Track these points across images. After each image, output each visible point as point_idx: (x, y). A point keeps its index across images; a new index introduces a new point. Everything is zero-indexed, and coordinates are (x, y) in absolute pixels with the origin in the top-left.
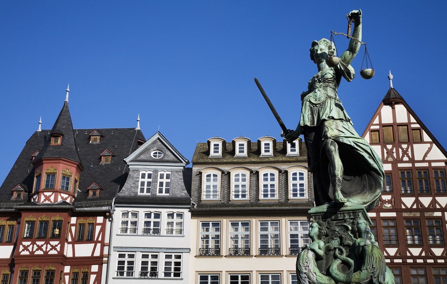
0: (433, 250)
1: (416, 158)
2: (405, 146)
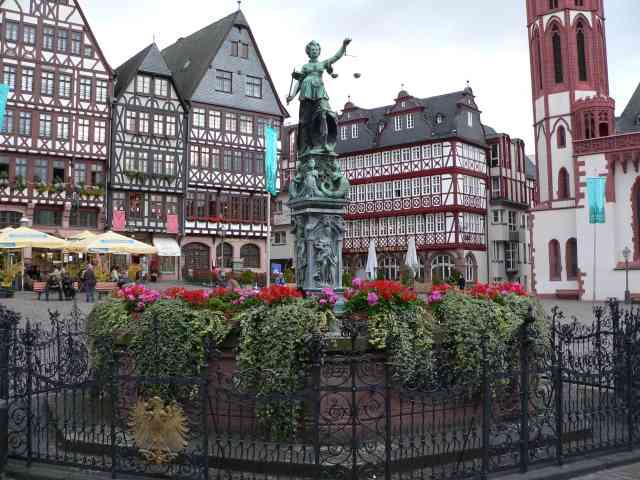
0: (62, 101)
1: (60, 18)
2: (52, 5)
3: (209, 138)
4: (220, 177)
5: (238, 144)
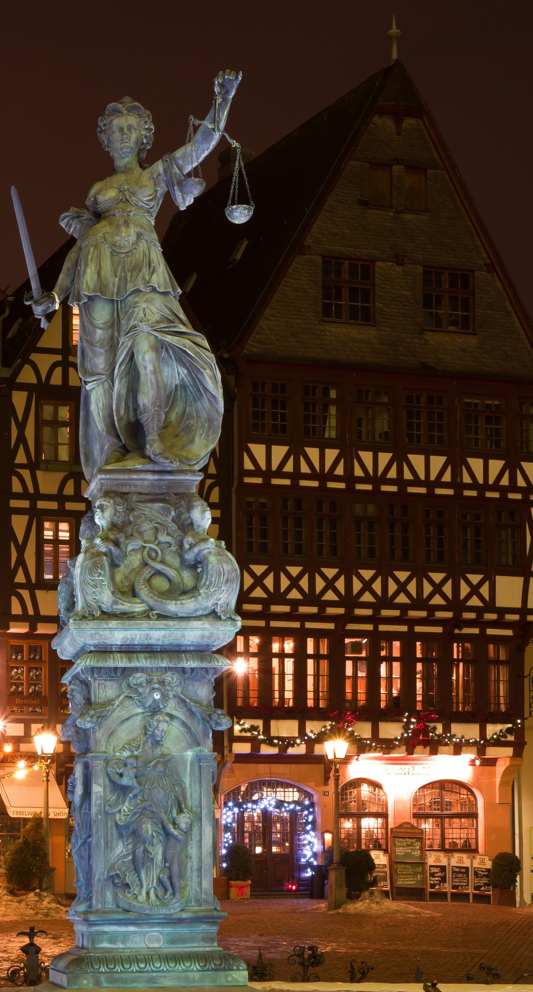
3: (305, 468)
4: (340, 584)
5: (400, 481)
